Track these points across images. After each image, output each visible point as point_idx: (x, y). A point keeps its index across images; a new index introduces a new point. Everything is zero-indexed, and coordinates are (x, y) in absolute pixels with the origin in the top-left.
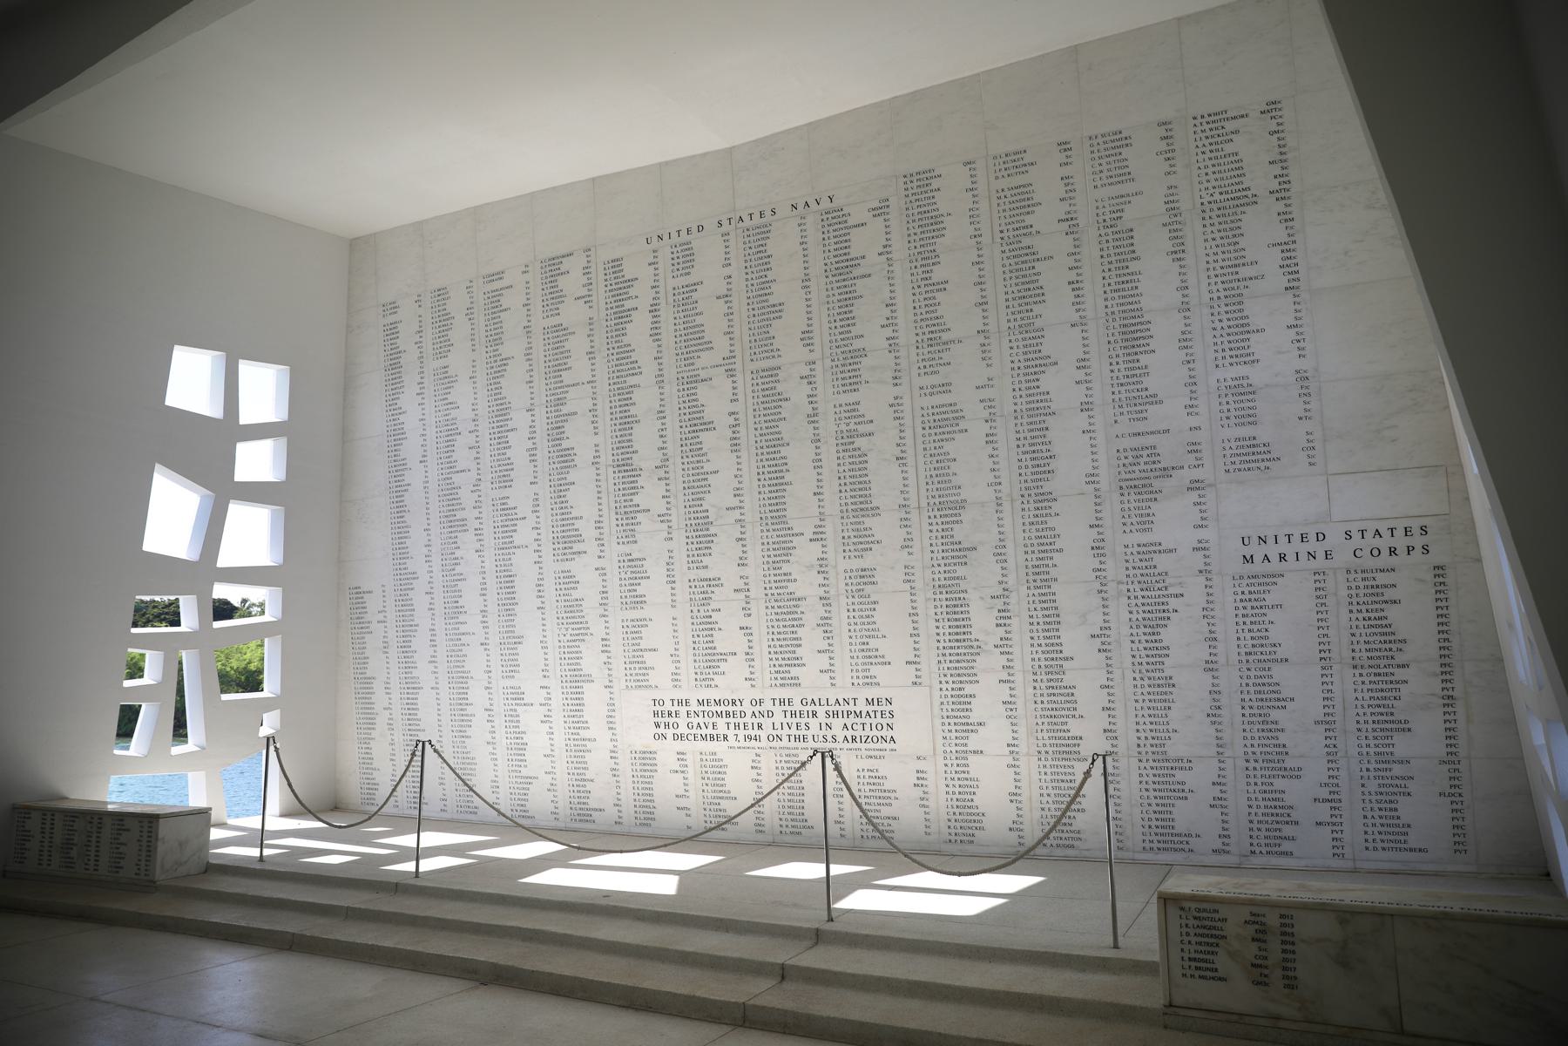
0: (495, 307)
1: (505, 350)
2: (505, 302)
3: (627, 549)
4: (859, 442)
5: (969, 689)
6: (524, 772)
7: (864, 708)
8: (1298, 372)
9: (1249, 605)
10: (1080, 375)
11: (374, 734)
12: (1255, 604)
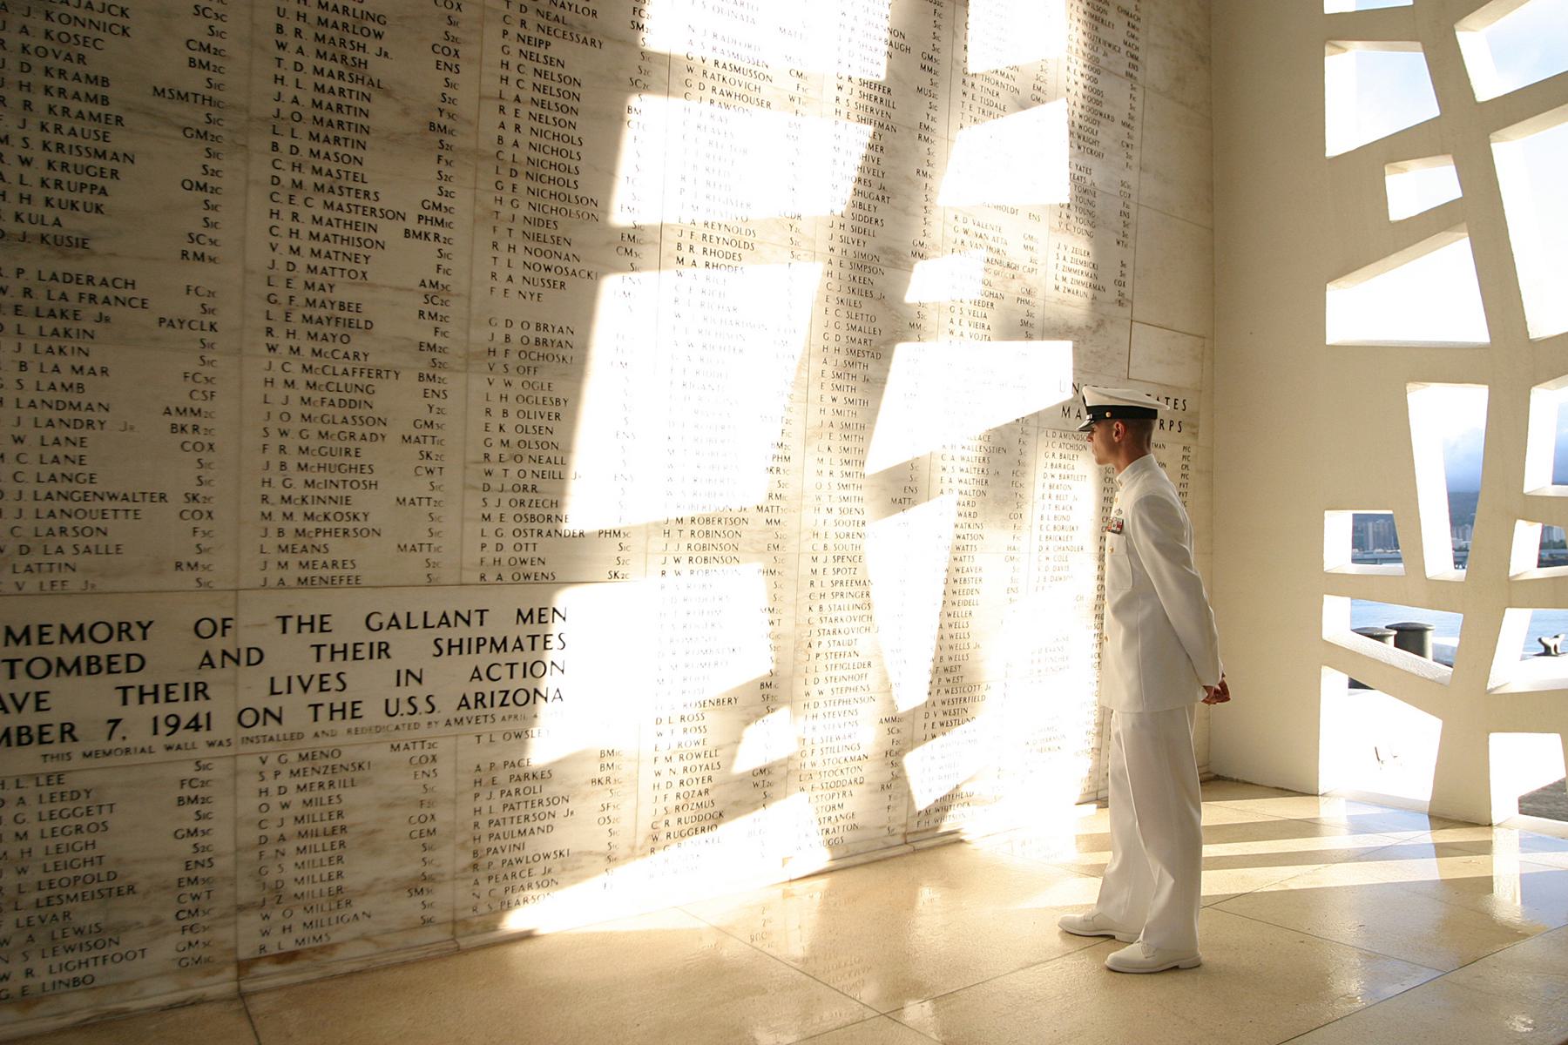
4: (558, 49)
9: (1057, 472)
12: (1063, 472)
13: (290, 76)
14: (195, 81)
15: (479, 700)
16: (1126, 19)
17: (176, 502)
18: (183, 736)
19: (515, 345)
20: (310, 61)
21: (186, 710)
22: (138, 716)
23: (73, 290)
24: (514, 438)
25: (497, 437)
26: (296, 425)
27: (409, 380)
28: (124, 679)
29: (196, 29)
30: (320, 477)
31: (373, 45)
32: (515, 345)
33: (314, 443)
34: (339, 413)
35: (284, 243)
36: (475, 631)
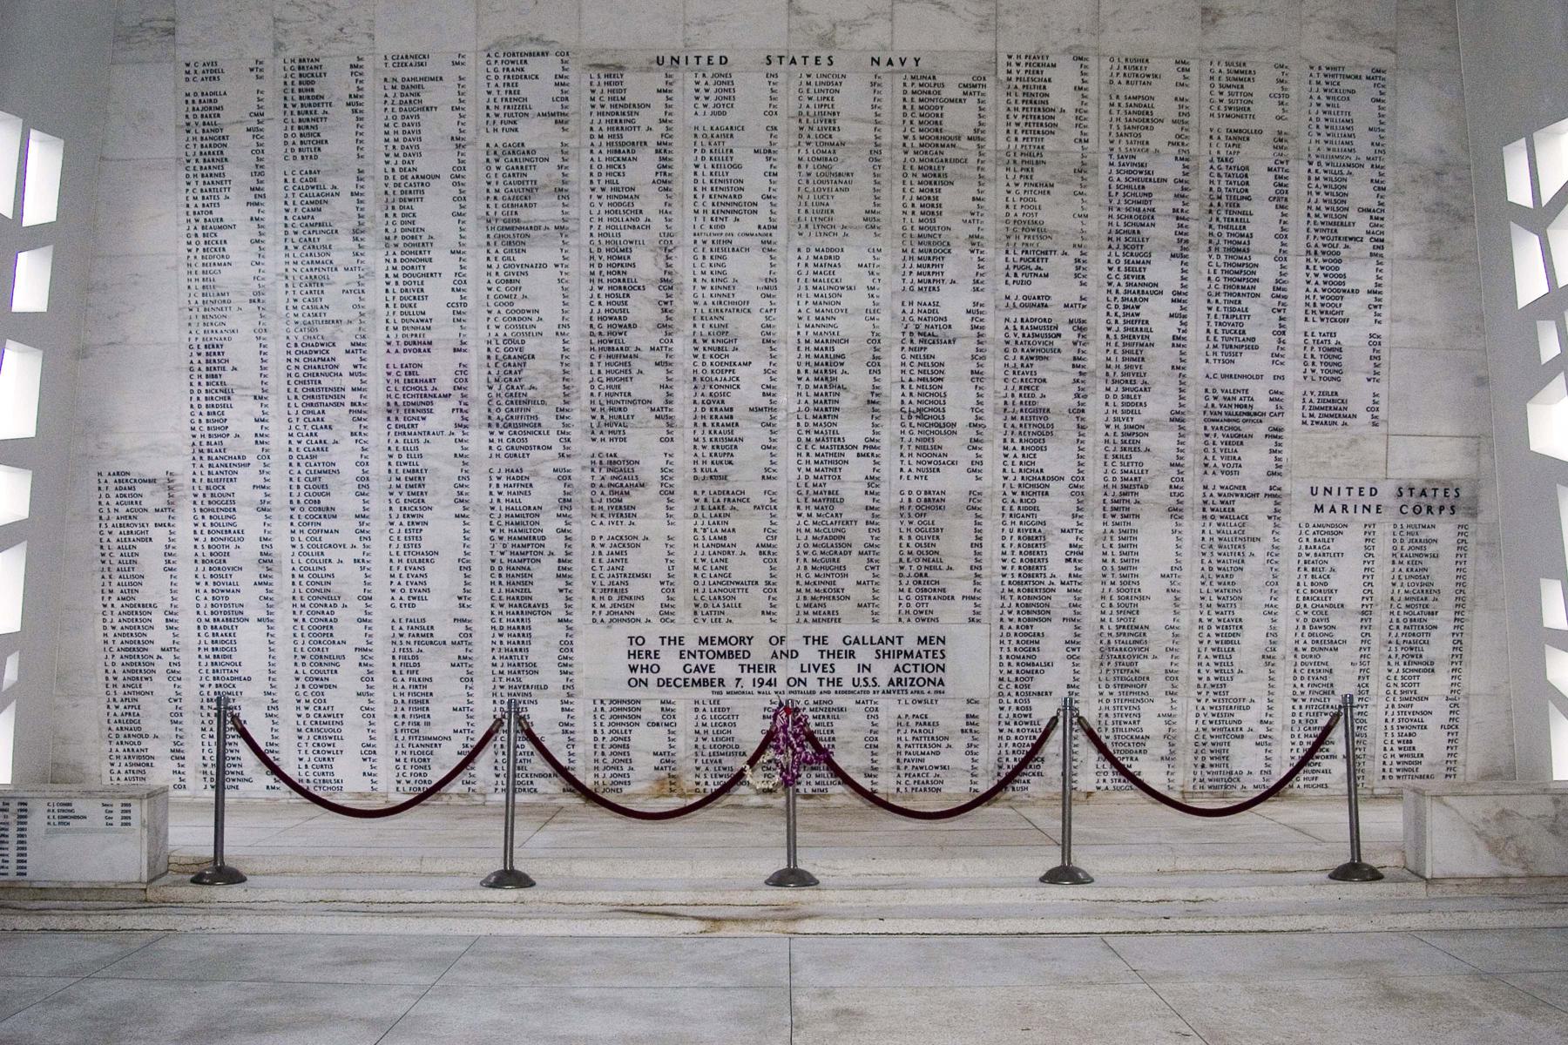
0: (409, 100)
1: (423, 166)
2: (426, 99)
3: (608, 447)
4: (931, 349)
5: (1038, 627)
6: (423, 731)
7: (916, 648)
8: (1371, 336)
9: (1312, 552)
10: (1176, 308)
11: (146, 686)
13: (804, 392)
14: (765, 402)
15: (899, 681)
16: (1367, 215)
17: (762, 585)
18: (765, 688)
19: (914, 503)
20: (812, 383)
21: (767, 677)
22: (748, 677)
23: (722, 498)
24: (914, 550)
25: (906, 550)
26: (811, 549)
27: (862, 525)
28: (742, 661)
29: (765, 380)
30: (822, 572)
31: (839, 369)
32: (914, 503)
33: (819, 557)
34: (830, 542)
35: (804, 467)
36: (897, 647)
